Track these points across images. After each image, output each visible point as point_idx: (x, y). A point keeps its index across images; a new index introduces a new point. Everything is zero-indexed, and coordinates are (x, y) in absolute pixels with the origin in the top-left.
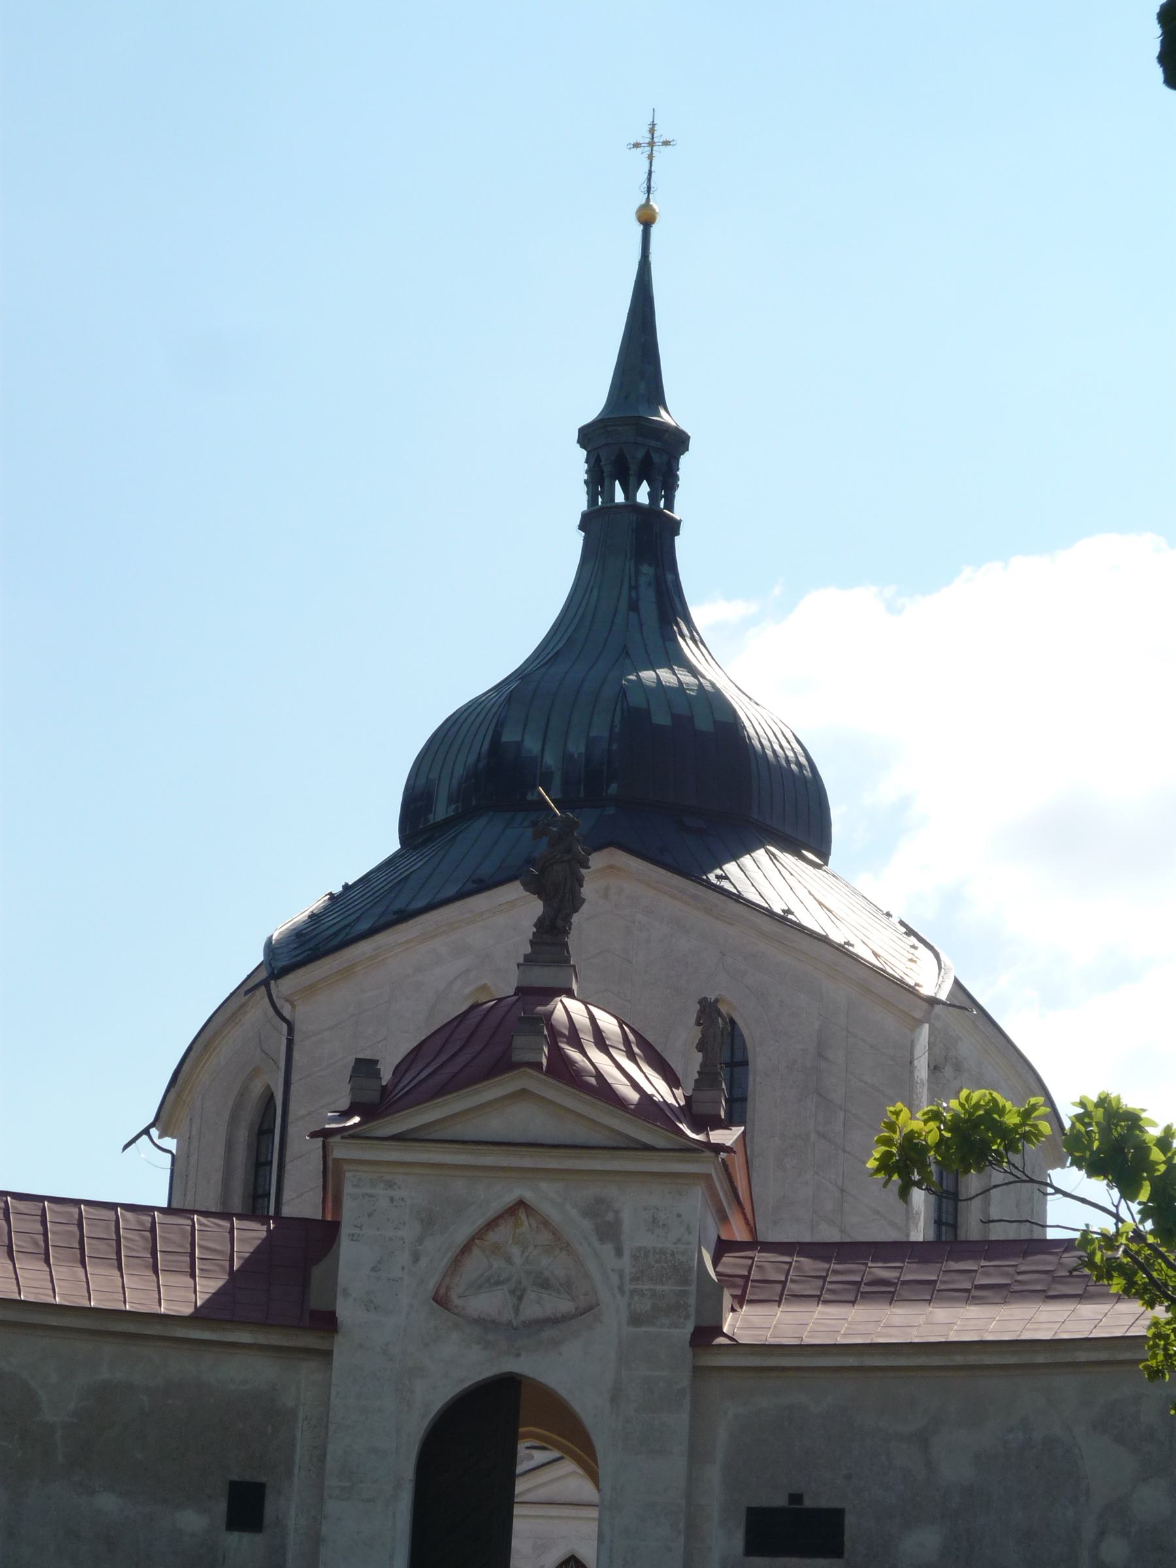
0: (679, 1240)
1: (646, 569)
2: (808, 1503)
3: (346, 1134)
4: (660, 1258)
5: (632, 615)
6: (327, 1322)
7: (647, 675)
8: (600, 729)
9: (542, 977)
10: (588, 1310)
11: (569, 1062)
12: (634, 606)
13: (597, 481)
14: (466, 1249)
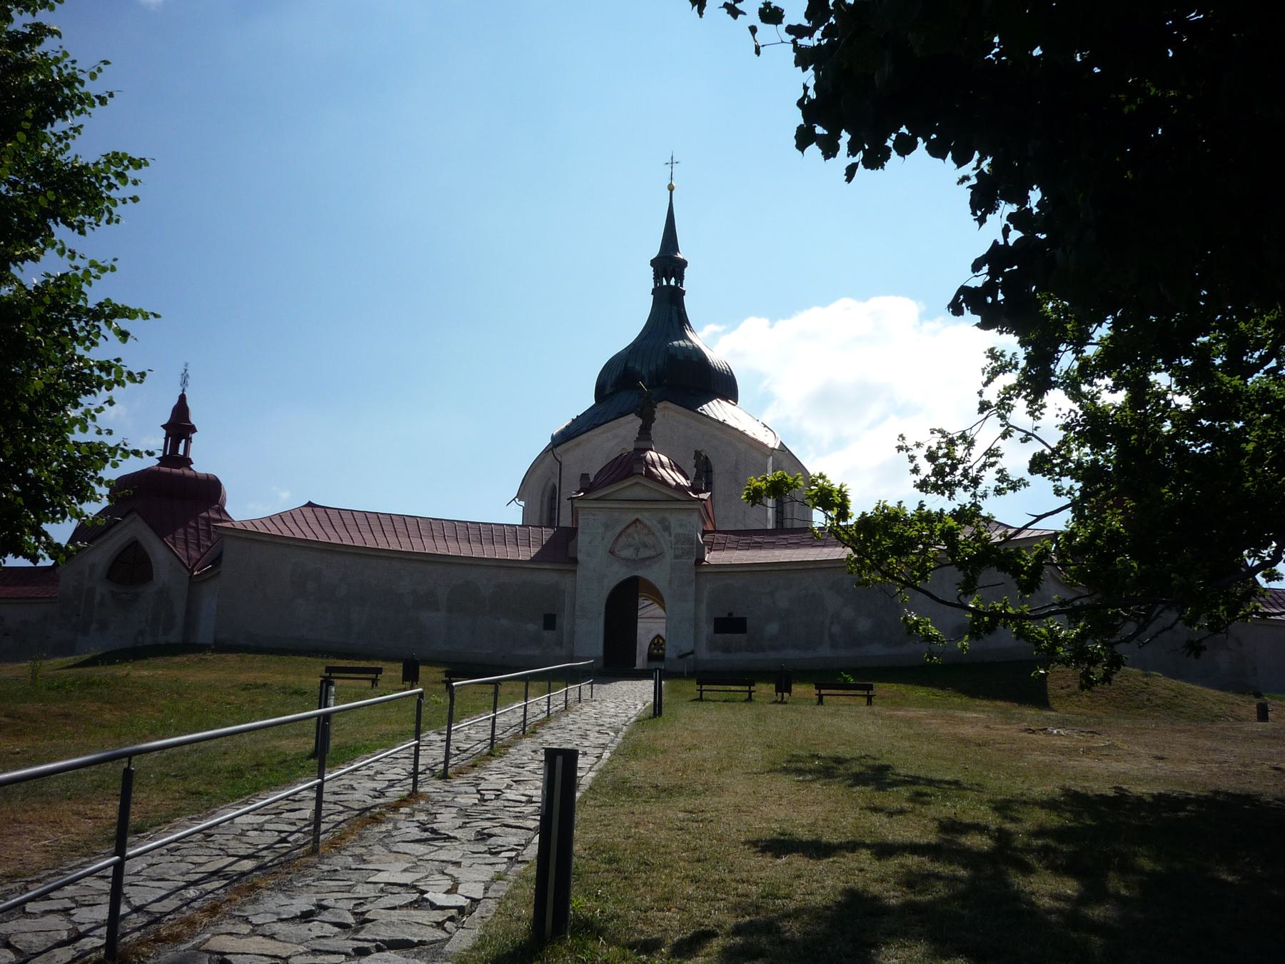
1: (675, 308)
2: (735, 616)
6: (575, 561)
7: (676, 343)
9: (642, 444)
10: (661, 554)
11: (653, 472)
12: (670, 320)
13: (657, 278)
14: (620, 535)
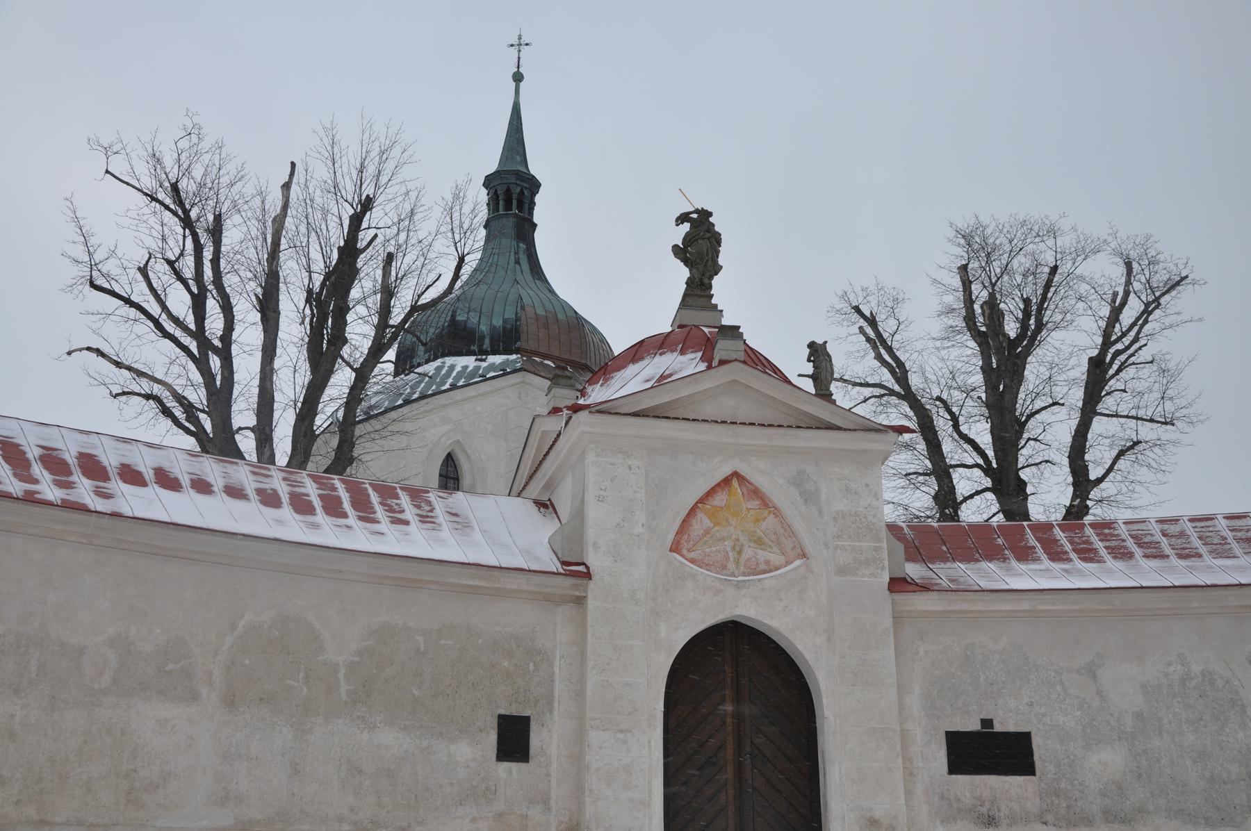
0: (869, 505)
2: (998, 728)
3: (593, 410)
4: (856, 519)
5: (517, 266)
12: (517, 262)
14: (692, 511)
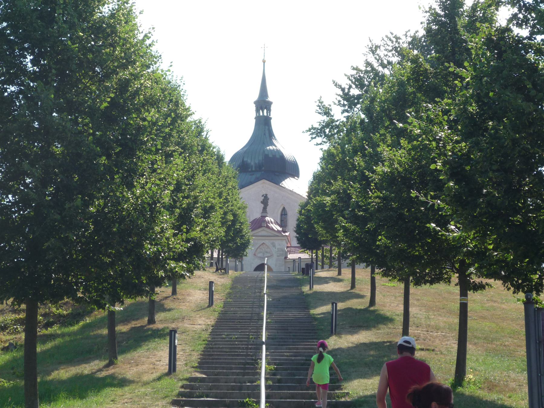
7: (268, 148)
8: (261, 158)
9: (264, 215)
11: (268, 226)
12: (265, 134)
13: (257, 111)
